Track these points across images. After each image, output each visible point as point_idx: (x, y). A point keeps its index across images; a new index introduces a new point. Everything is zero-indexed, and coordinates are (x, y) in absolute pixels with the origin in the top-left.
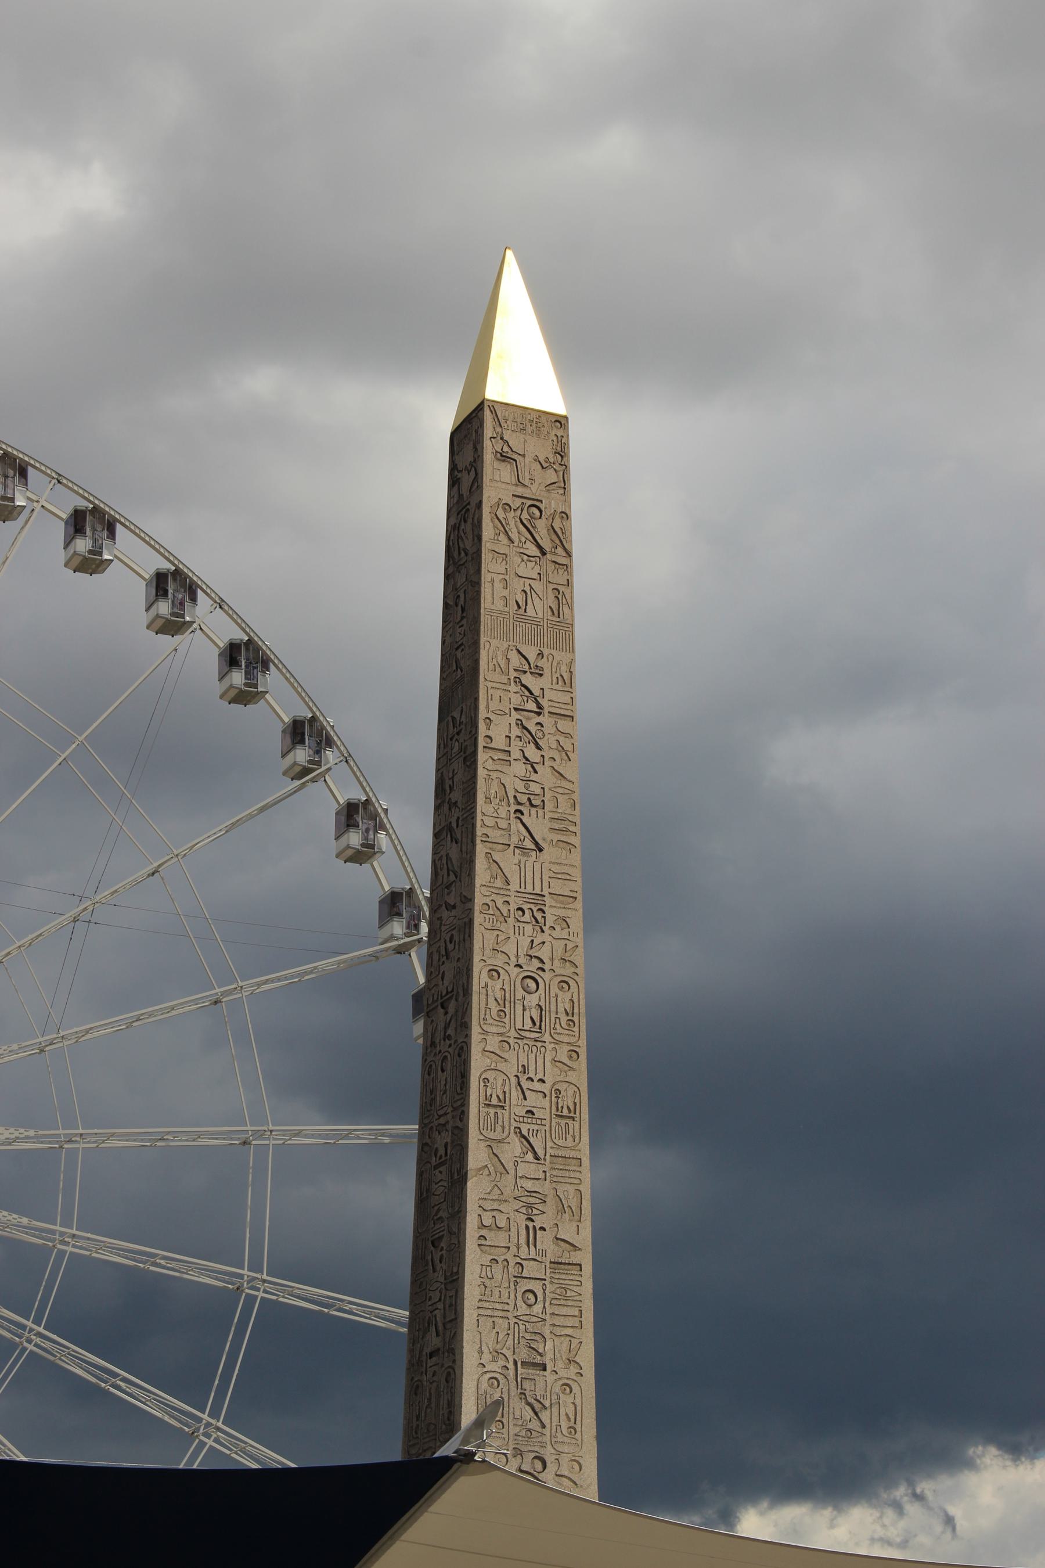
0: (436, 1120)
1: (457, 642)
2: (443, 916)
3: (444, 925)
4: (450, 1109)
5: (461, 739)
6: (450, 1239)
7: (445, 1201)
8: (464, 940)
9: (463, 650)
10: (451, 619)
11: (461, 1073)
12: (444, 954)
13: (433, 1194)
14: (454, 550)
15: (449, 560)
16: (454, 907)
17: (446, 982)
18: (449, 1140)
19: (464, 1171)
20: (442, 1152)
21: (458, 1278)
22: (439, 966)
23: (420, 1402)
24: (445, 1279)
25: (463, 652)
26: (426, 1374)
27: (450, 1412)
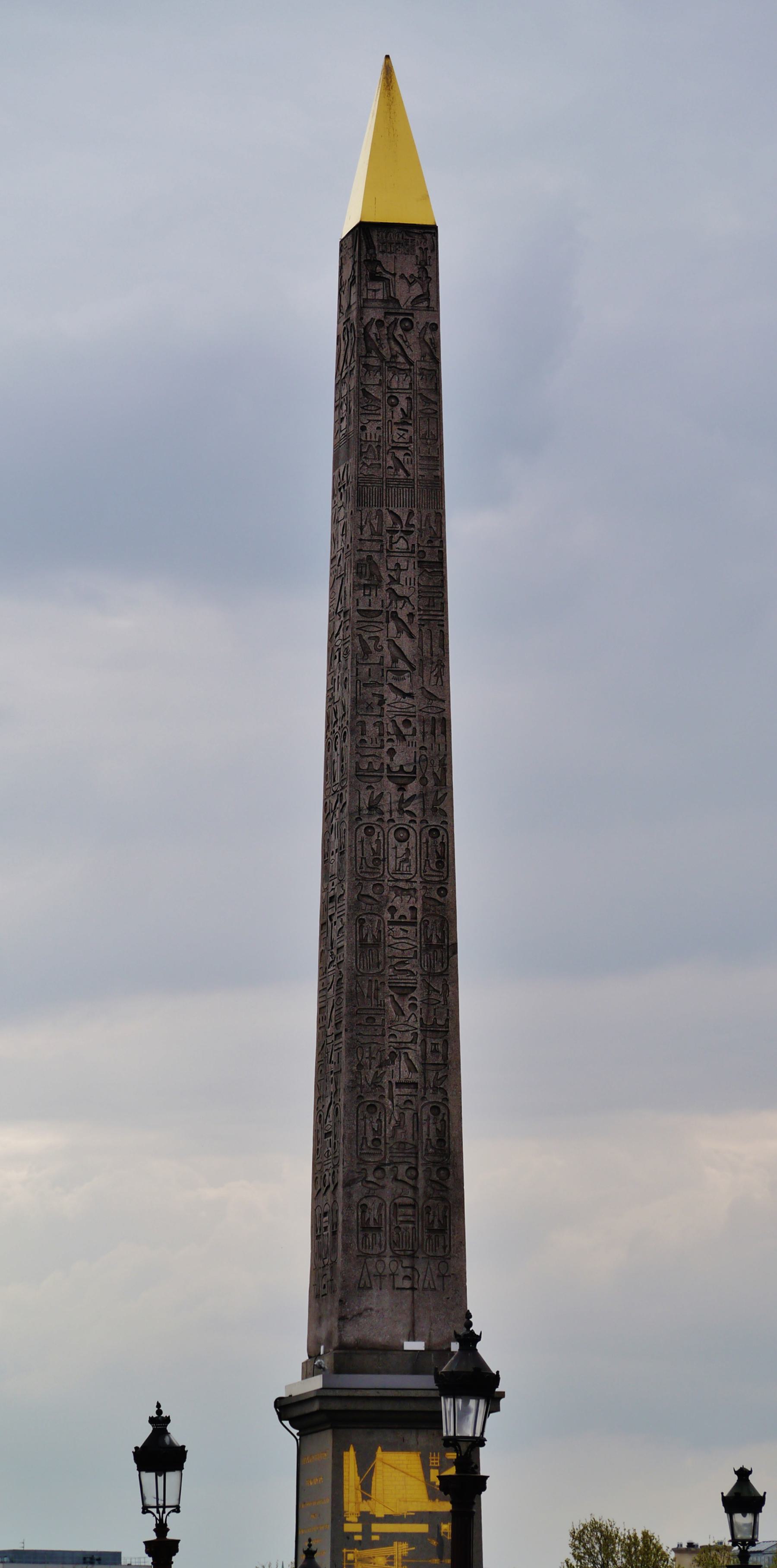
0: (388, 881)
1: (393, 441)
2: (386, 696)
3: (388, 705)
4: (418, 879)
5: (413, 538)
6: (429, 994)
7: (415, 957)
8: (433, 733)
9: (406, 454)
10: (377, 412)
11: (437, 852)
12: (391, 730)
13: (389, 946)
14: (381, 345)
15: (369, 351)
16: (410, 695)
17: (398, 760)
18: (419, 906)
19: (451, 942)
20: (408, 915)
21: (448, 1031)
22: (382, 740)
23: (379, 1120)
24: (421, 1026)
25: (407, 457)
26: (391, 1098)
27: (441, 1140)
